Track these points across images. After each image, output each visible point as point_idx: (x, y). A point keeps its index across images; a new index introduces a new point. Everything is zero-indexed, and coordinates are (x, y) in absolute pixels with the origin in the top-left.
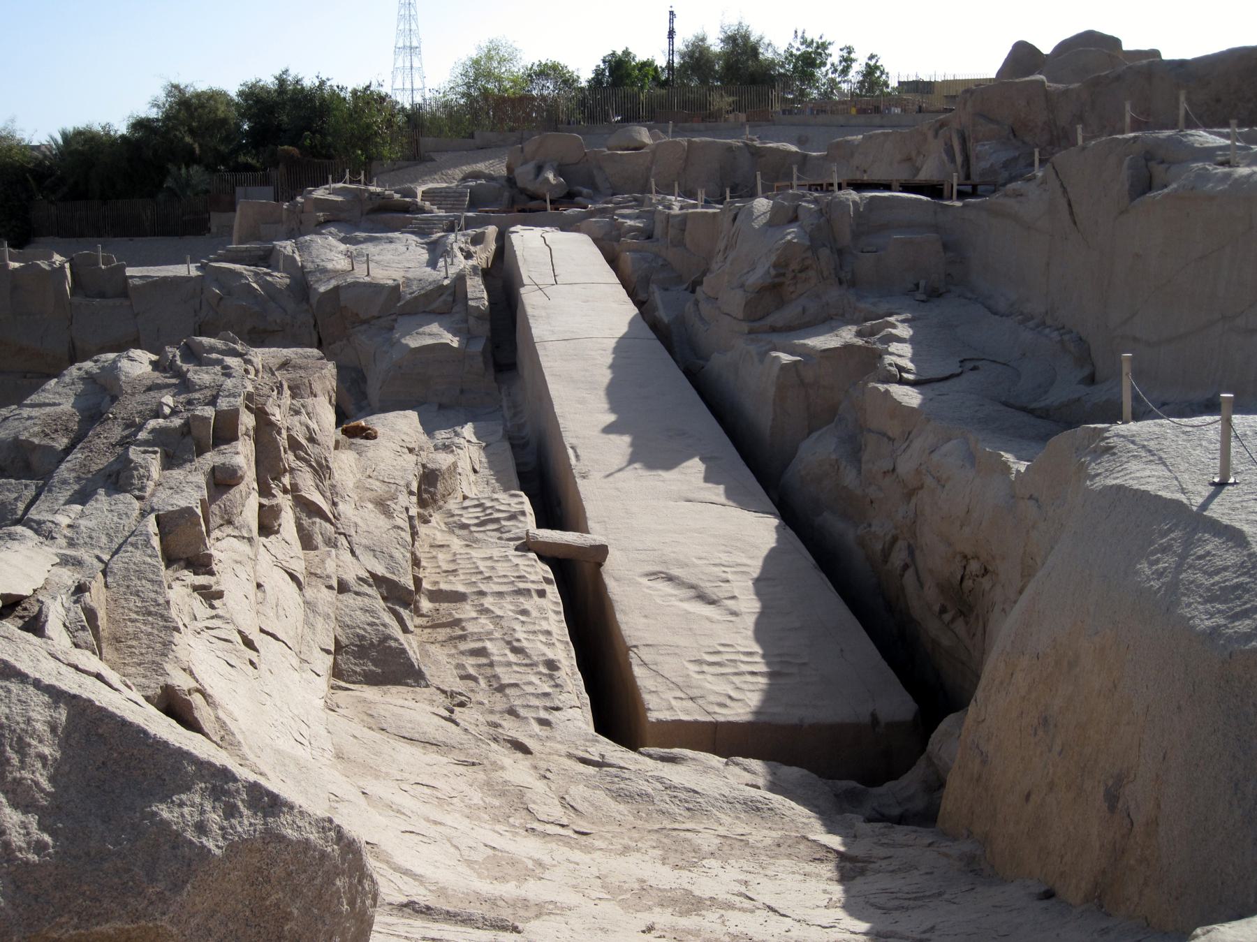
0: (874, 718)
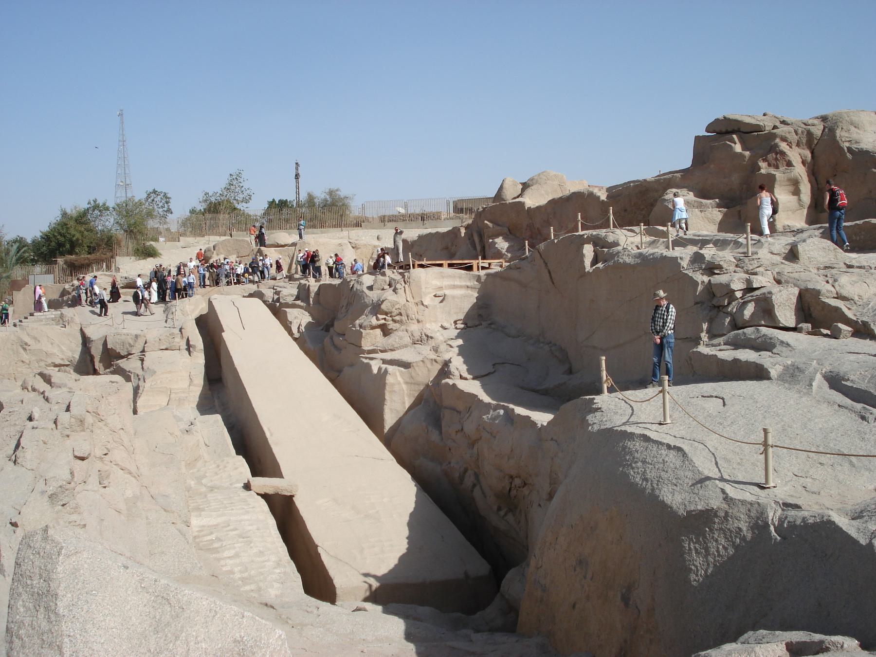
0: (466, 574)
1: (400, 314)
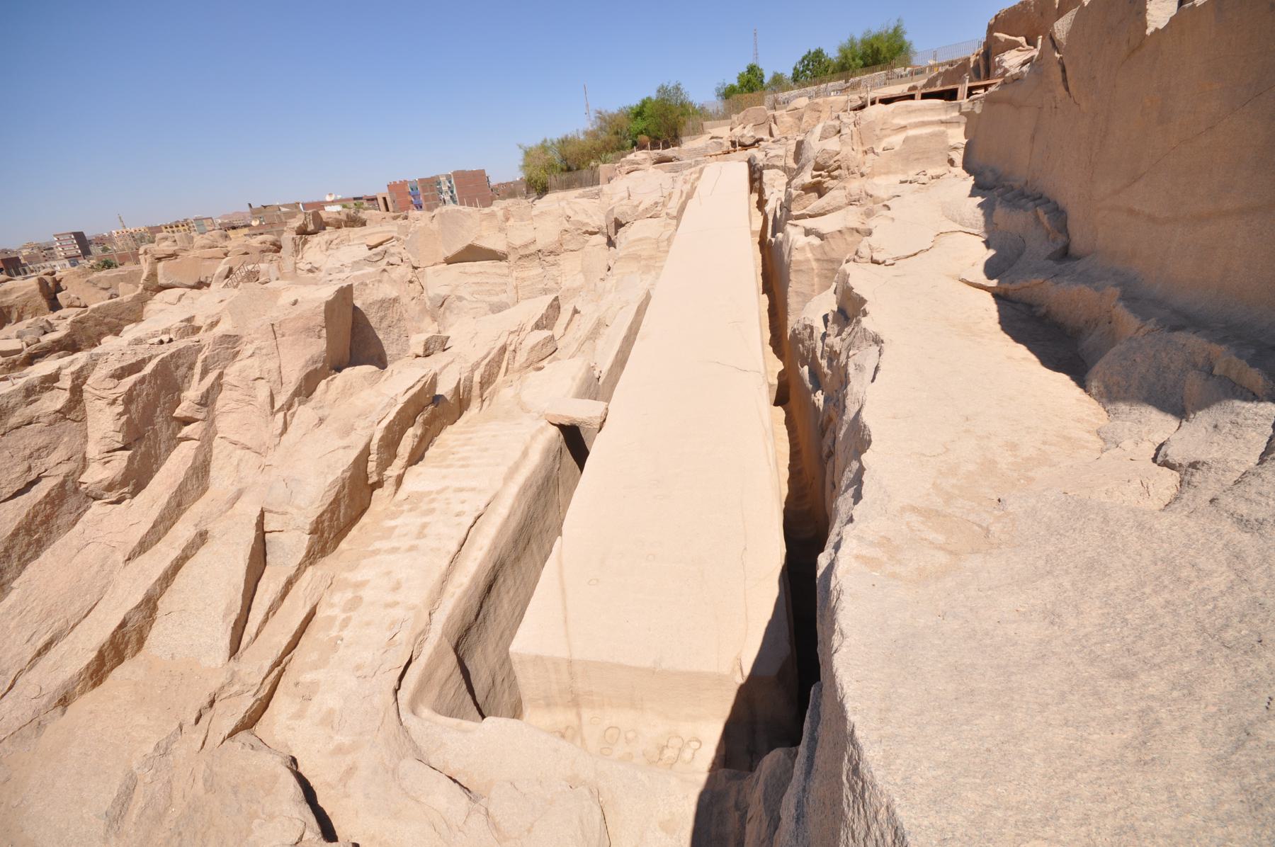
1: (839, 167)
